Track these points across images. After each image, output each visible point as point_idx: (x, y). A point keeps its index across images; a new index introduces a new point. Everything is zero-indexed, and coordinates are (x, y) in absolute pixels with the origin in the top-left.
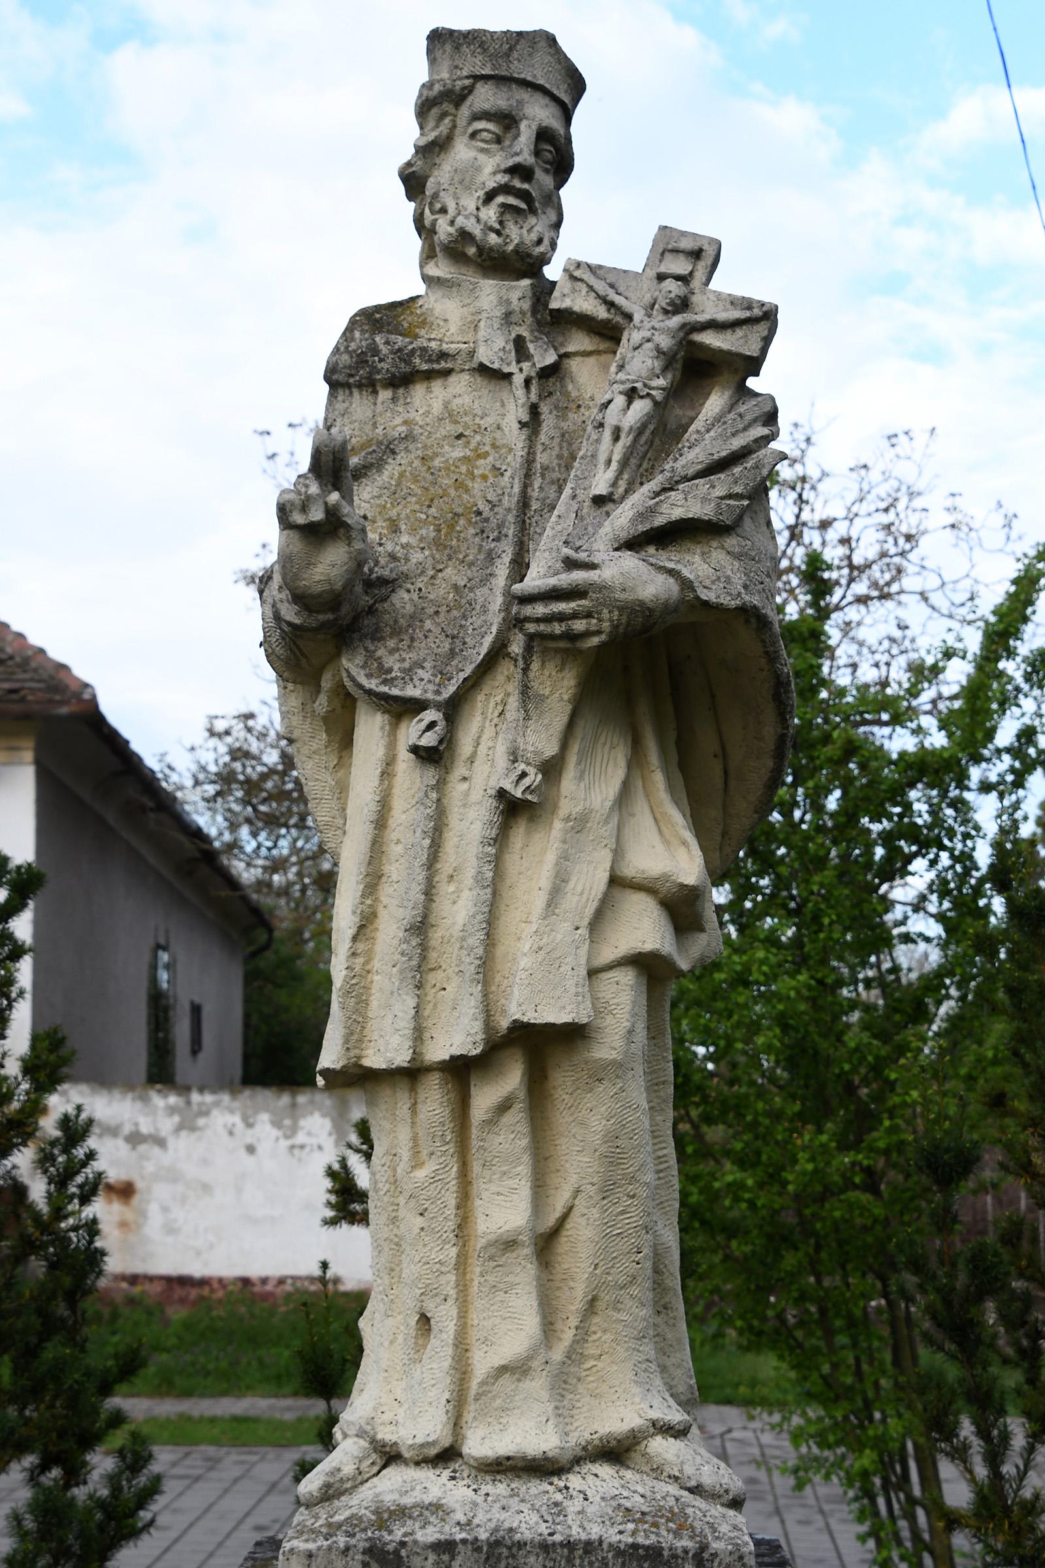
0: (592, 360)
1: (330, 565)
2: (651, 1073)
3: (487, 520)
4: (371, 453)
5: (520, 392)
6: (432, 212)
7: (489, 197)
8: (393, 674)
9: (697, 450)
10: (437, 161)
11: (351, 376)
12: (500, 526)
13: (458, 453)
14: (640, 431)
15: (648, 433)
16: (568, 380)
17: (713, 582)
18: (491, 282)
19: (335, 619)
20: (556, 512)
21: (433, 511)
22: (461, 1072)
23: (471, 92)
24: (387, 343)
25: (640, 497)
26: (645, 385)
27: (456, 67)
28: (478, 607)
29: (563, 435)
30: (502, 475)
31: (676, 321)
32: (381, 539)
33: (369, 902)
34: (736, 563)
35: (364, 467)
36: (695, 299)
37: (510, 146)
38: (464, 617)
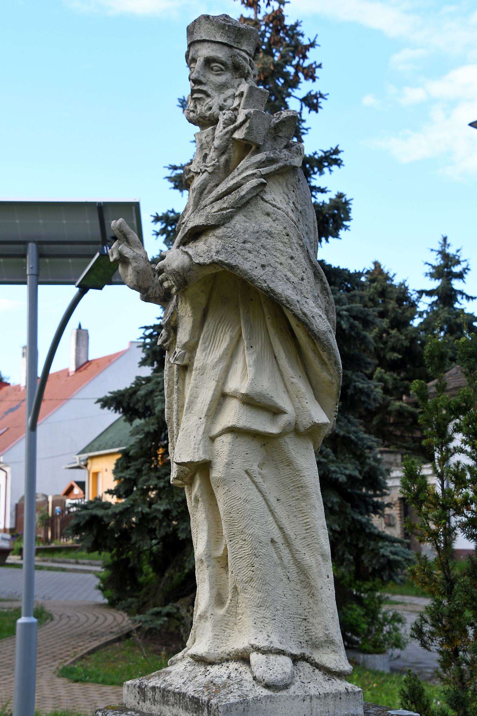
34: (220, 241)
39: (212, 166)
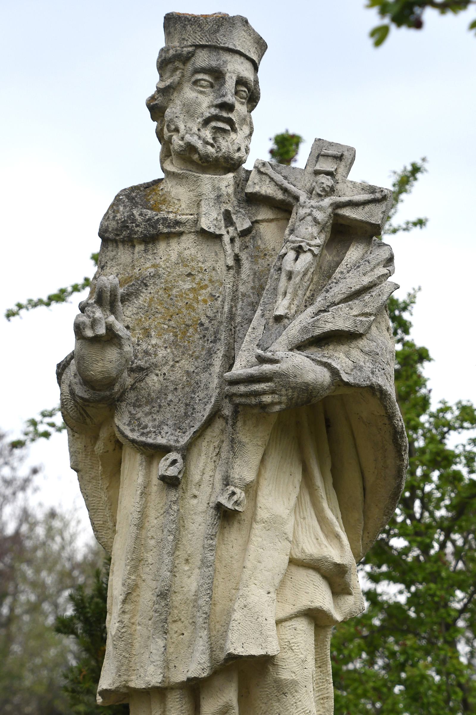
0: (273, 225)
1: (108, 361)
2: (318, 691)
3: (207, 329)
4: (131, 286)
5: (228, 247)
6: (169, 131)
7: (206, 122)
8: (148, 430)
9: (341, 285)
10: (172, 98)
11: (117, 235)
12: (216, 333)
13: (188, 286)
14: (305, 274)
15: (309, 274)
16: (258, 238)
17: (352, 370)
18: (208, 176)
19: (111, 395)
20: (251, 326)
21: (172, 323)
22: (194, 689)
23: (193, 55)
24: (141, 214)
25: (305, 317)
26: (308, 244)
27: (184, 39)
28: (202, 385)
29: (255, 274)
30: (216, 300)
31: (327, 201)
32: (138, 341)
33: (133, 577)
35: (127, 294)
36: (338, 187)
37: (219, 90)
38: (194, 392)
39: (319, 246)
